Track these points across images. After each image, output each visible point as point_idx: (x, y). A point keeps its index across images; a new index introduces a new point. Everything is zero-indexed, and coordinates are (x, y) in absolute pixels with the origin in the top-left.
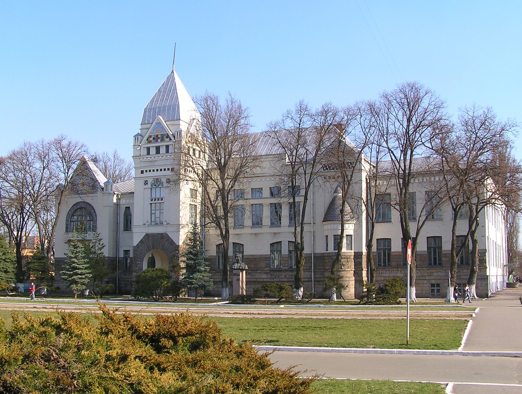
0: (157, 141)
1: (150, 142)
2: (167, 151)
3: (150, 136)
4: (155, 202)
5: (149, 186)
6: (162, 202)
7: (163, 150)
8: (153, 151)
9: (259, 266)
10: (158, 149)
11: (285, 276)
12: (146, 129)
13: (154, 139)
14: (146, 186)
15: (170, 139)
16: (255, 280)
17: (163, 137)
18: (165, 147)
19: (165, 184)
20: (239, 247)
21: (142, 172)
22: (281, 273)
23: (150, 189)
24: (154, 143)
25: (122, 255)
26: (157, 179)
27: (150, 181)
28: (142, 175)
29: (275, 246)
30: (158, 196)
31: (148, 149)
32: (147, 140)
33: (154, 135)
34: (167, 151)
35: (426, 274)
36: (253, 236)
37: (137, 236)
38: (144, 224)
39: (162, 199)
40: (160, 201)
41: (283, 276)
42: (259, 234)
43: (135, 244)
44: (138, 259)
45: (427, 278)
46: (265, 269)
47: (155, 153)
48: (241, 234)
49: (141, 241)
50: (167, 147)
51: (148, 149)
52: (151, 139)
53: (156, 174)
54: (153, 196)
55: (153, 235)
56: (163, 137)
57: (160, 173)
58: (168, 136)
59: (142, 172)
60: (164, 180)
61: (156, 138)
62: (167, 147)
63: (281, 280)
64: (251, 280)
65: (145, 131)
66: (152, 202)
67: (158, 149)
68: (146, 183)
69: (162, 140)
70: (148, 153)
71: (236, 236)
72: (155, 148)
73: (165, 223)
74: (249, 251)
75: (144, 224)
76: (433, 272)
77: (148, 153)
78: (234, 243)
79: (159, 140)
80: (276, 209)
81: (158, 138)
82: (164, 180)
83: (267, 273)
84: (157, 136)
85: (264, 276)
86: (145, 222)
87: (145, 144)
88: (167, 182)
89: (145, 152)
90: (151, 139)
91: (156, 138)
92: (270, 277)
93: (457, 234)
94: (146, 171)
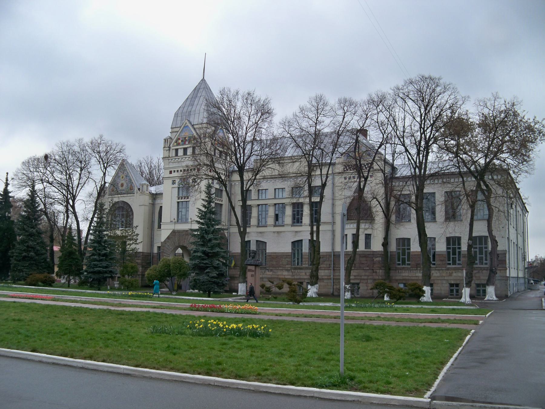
0: (185, 144)
5: (176, 185)
6: (188, 200)
8: (181, 153)
9: (281, 263)
11: (306, 273)
12: (176, 132)
13: (182, 141)
14: (174, 186)
16: (277, 276)
20: (261, 244)
21: (171, 172)
22: (301, 271)
23: (177, 189)
24: (183, 145)
25: (155, 251)
27: (177, 181)
29: (297, 244)
30: (185, 194)
31: (177, 150)
32: (176, 142)
35: (444, 275)
36: (276, 234)
37: (164, 234)
38: (171, 222)
39: (188, 198)
41: (304, 274)
42: (281, 232)
43: (163, 238)
44: (165, 254)
45: (446, 278)
46: (287, 266)
48: (264, 232)
49: (168, 238)
52: (180, 141)
54: (181, 195)
55: (179, 232)
59: (171, 172)
63: (302, 277)
64: (272, 276)
65: (175, 134)
66: (179, 201)
68: (174, 182)
70: (177, 154)
71: (260, 235)
72: (182, 150)
73: (190, 220)
74: (271, 249)
76: (452, 273)
77: (177, 154)
78: (257, 241)
79: (187, 143)
80: (297, 208)
81: (186, 140)
83: (288, 270)
84: (185, 138)
85: (285, 273)
86: (172, 220)
89: (173, 153)
90: (180, 141)
91: (184, 141)
92: (291, 274)
93: (474, 235)
94: (174, 171)
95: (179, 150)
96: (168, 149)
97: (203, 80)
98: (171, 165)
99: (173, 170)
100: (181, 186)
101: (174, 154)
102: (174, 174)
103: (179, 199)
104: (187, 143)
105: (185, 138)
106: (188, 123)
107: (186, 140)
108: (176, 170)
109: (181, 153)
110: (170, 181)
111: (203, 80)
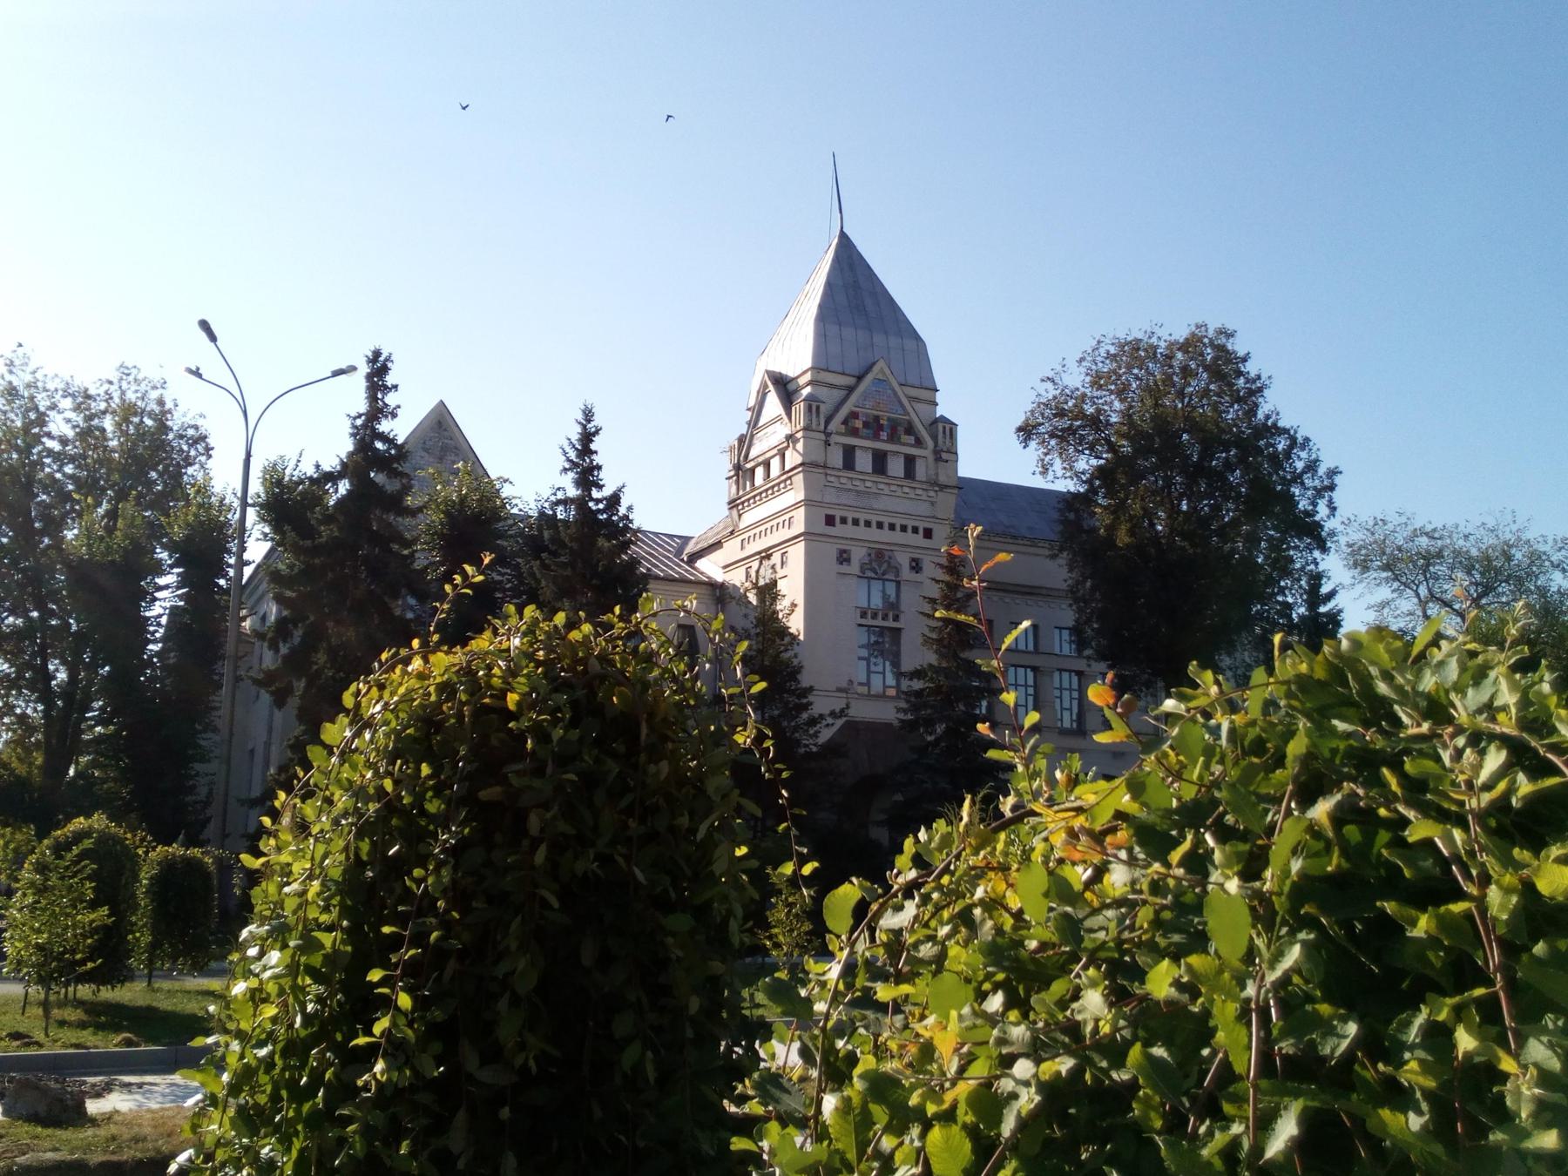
0: (876, 437)
1: (854, 432)
2: (910, 473)
3: (854, 415)
4: (885, 624)
5: (854, 568)
7: (896, 467)
8: (864, 462)
13: (866, 425)
14: (844, 568)
15: (919, 443)
18: (902, 460)
19: (906, 573)
21: (830, 521)
27: (858, 554)
31: (849, 453)
32: (845, 422)
33: (867, 415)
34: (910, 473)
38: (839, 690)
39: (896, 618)
40: (890, 623)
50: (910, 461)
51: (849, 453)
53: (874, 534)
57: (885, 536)
58: (910, 430)
60: (903, 560)
61: (874, 427)
62: (910, 461)
66: (863, 621)
68: (843, 557)
69: (893, 438)
70: (849, 463)
75: (839, 690)
77: (849, 463)
79: (884, 435)
81: (881, 428)
82: (903, 560)
84: (877, 418)
86: (844, 685)
88: (912, 568)
89: (836, 458)
90: (858, 424)
91: (874, 427)
94: (844, 521)
95: (858, 453)
96: (823, 437)
97: (845, 244)
98: (831, 496)
99: (838, 514)
100: (869, 574)
102: (838, 530)
103: (863, 615)
104: (884, 435)
106: (887, 371)
107: (881, 428)
109: (864, 462)
110: (831, 550)
111: (845, 244)
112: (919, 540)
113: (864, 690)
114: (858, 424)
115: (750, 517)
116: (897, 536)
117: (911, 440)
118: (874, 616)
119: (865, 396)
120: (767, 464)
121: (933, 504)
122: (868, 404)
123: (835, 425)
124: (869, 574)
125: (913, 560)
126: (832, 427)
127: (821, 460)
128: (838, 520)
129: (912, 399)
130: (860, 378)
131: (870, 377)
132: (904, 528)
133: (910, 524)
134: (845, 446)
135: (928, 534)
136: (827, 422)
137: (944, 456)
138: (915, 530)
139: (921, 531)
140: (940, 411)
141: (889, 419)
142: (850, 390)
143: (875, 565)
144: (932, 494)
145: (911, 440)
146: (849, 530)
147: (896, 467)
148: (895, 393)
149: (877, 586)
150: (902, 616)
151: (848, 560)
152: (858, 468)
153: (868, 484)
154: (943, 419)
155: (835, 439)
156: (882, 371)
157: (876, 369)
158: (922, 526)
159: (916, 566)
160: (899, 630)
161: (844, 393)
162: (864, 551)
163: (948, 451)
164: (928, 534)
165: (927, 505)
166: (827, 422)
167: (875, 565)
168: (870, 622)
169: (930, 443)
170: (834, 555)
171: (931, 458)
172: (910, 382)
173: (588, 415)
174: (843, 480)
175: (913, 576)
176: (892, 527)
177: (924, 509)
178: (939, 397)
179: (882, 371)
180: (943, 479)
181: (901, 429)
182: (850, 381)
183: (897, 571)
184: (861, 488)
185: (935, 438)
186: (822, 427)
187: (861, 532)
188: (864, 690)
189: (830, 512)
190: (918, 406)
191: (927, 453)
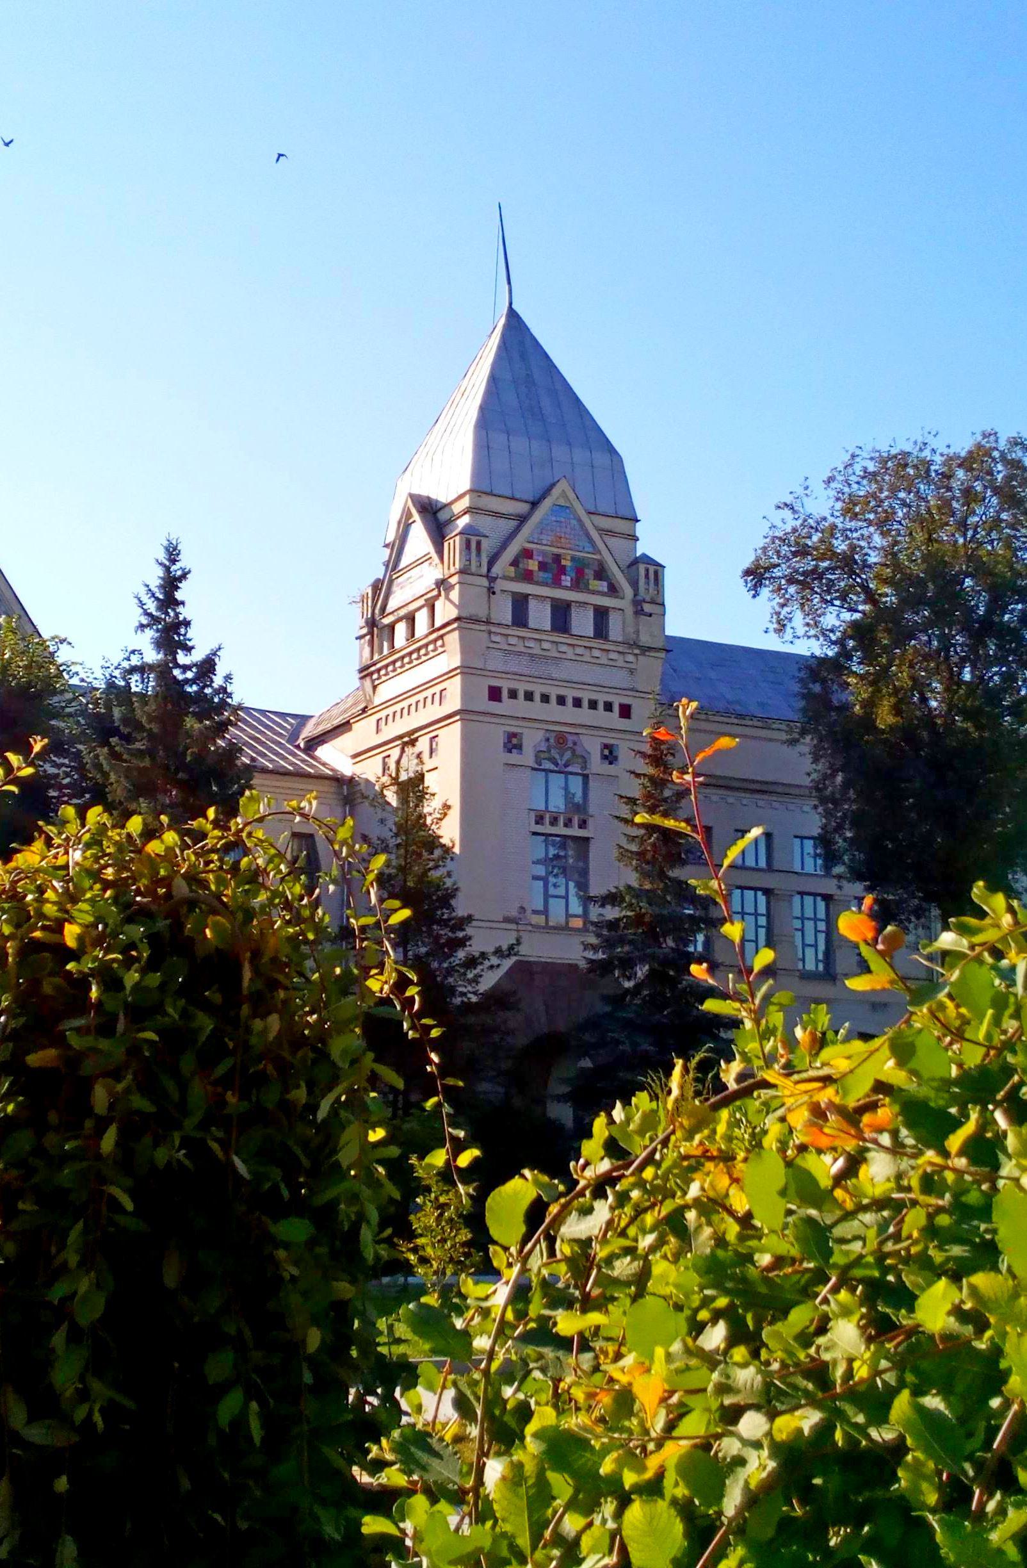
0: (556, 583)
1: (528, 577)
2: (601, 632)
3: (527, 554)
5: (527, 757)
7: (582, 622)
8: (540, 615)
10: (561, 615)
13: (543, 566)
14: (514, 758)
15: (613, 590)
17: (580, 572)
18: (591, 614)
19: (596, 764)
21: (495, 694)
26: (561, 739)
27: (532, 739)
28: (494, 707)
31: (520, 603)
32: (515, 563)
33: (544, 553)
34: (601, 632)
38: (507, 920)
39: (583, 824)
40: (575, 831)
47: (548, 627)
50: (601, 614)
51: (520, 603)
53: (553, 712)
56: (580, 572)
57: (569, 714)
58: (601, 573)
60: (592, 746)
61: (554, 569)
62: (601, 614)
66: (539, 829)
67: (561, 615)
68: (513, 743)
69: (579, 584)
70: (520, 618)
75: (507, 920)
77: (520, 618)
79: (567, 580)
81: (562, 570)
82: (592, 746)
84: (557, 558)
86: (514, 913)
87: (505, 578)
88: (605, 757)
89: (504, 611)
90: (533, 565)
91: (554, 569)
94: (513, 694)
95: (532, 603)
96: (485, 582)
98: (496, 662)
99: (505, 685)
100: (548, 765)
101: (508, 618)
102: (506, 706)
103: (539, 820)
104: (567, 580)
105: (557, 558)
106: (571, 495)
107: (562, 570)
108: (522, 688)
112: (613, 719)
113: (540, 920)
114: (533, 565)
115: (388, 690)
116: (584, 715)
117: (603, 586)
118: (554, 821)
119: (542, 528)
120: (411, 619)
121: (632, 672)
122: (545, 539)
123: (502, 566)
124: (548, 765)
125: (606, 746)
126: (497, 570)
127: (483, 615)
128: (505, 694)
129: (605, 532)
130: (534, 504)
131: (547, 503)
132: (593, 705)
133: (601, 699)
134: (514, 594)
135: (625, 711)
136: (491, 564)
137: (647, 608)
138: (608, 707)
139: (616, 708)
140: (641, 549)
141: (573, 559)
142: (522, 519)
143: (555, 753)
144: (630, 658)
145: (603, 586)
146: (520, 707)
147: (582, 622)
148: (580, 520)
149: (557, 781)
150: (590, 822)
151: (519, 747)
152: (531, 624)
153: (546, 645)
154: (646, 559)
155: (500, 585)
156: (564, 494)
157: (556, 492)
158: (617, 701)
159: (610, 755)
160: (587, 839)
161: (515, 523)
162: (540, 735)
163: (653, 602)
164: (625, 711)
165: (624, 674)
166: (491, 564)
167: (555, 753)
168: (547, 829)
169: (628, 591)
170: (501, 740)
171: (630, 610)
172: (601, 510)
173: (173, 553)
174: (513, 641)
175: (606, 769)
176: (577, 703)
177: (620, 678)
178: (640, 529)
179: (564, 494)
180: (645, 640)
181: (589, 573)
182: (523, 508)
183: (585, 761)
184: (537, 651)
185: (634, 584)
186: (484, 570)
187: (536, 709)
188: (540, 920)
189: (496, 683)
190: (612, 542)
191: (625, 603)
